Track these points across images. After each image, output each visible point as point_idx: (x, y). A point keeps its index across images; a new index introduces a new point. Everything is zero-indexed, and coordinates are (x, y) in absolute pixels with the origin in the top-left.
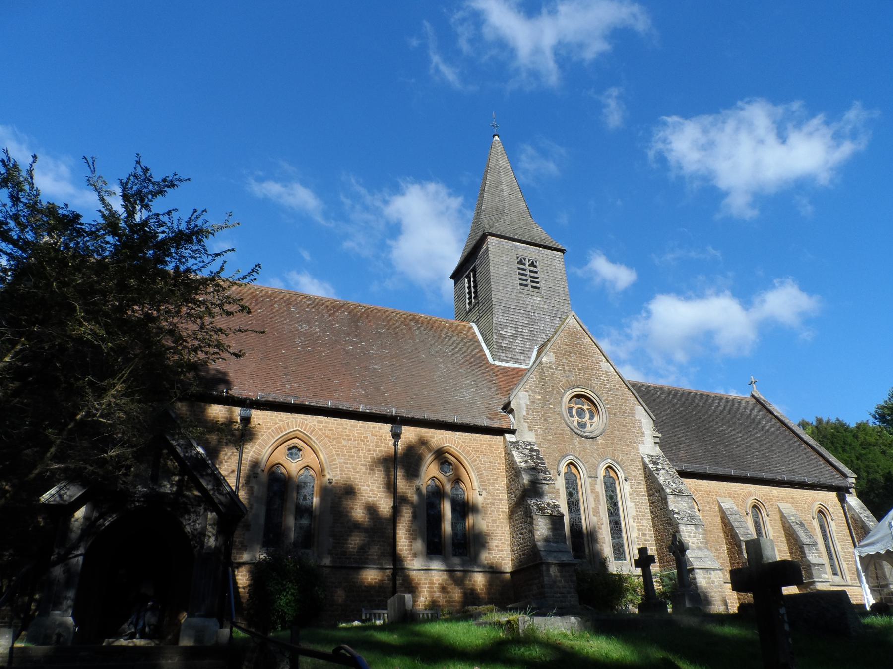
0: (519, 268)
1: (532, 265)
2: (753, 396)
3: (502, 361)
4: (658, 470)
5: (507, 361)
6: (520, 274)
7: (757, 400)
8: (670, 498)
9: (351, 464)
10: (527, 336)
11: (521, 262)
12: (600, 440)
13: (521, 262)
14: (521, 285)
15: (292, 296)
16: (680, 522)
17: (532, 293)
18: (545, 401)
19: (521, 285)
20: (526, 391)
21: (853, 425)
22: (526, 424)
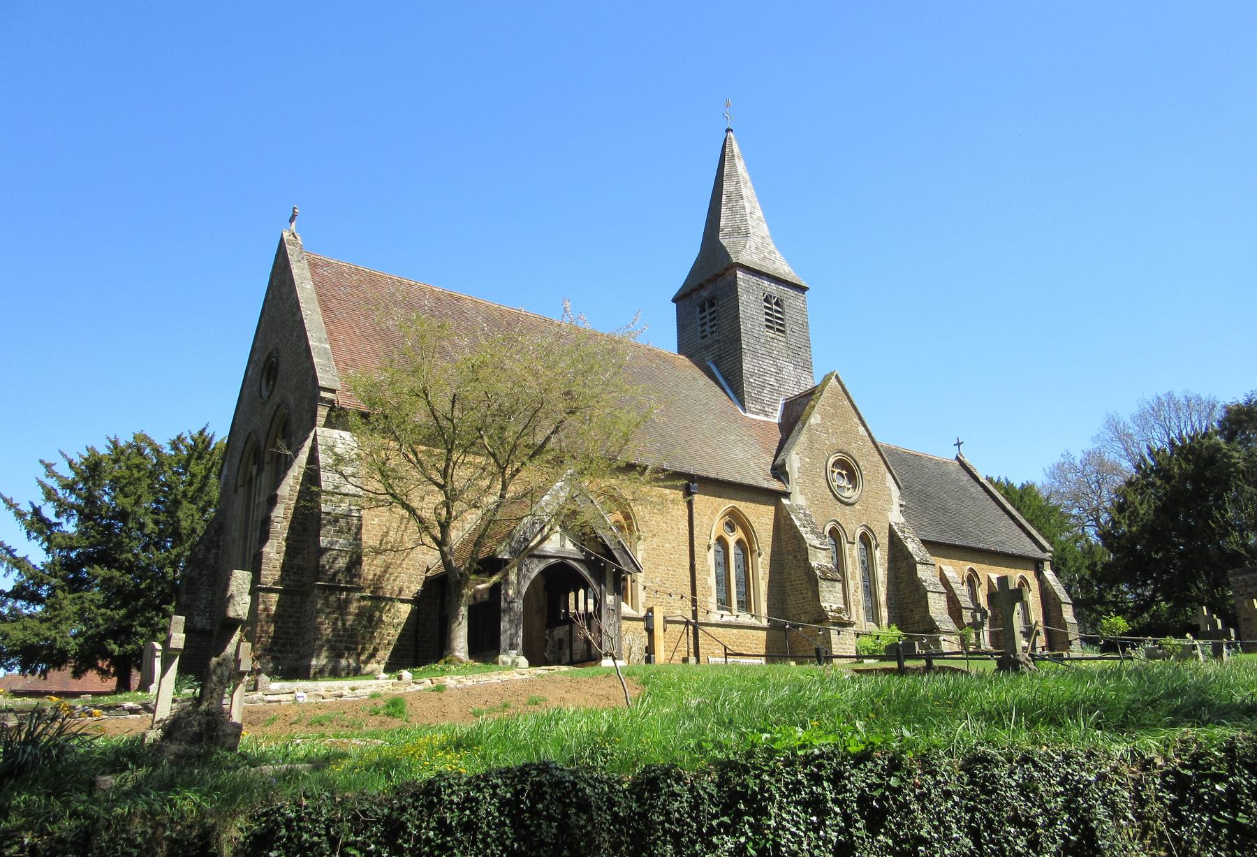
0: (766, 307)
1: (777, 304)
2: (957, 458)
3: (753, 413)
4: (905, 537)
5: (757, 414)
6: (766, 313)
7: (963, 464)
8: (919, 567)
9: (655, 521)
10: (773, 385)
11: (766, 300)
12: (857, 507)
13: (766, 300)
14: (767, 326)
15: (539, 320)
16: (928, 589)
17: (778, 337)
18: (812, 464)
19: (767, 326)
20: (797, 454)
21: (1018, 485)
22: (798, 487)
